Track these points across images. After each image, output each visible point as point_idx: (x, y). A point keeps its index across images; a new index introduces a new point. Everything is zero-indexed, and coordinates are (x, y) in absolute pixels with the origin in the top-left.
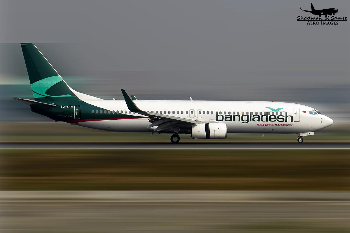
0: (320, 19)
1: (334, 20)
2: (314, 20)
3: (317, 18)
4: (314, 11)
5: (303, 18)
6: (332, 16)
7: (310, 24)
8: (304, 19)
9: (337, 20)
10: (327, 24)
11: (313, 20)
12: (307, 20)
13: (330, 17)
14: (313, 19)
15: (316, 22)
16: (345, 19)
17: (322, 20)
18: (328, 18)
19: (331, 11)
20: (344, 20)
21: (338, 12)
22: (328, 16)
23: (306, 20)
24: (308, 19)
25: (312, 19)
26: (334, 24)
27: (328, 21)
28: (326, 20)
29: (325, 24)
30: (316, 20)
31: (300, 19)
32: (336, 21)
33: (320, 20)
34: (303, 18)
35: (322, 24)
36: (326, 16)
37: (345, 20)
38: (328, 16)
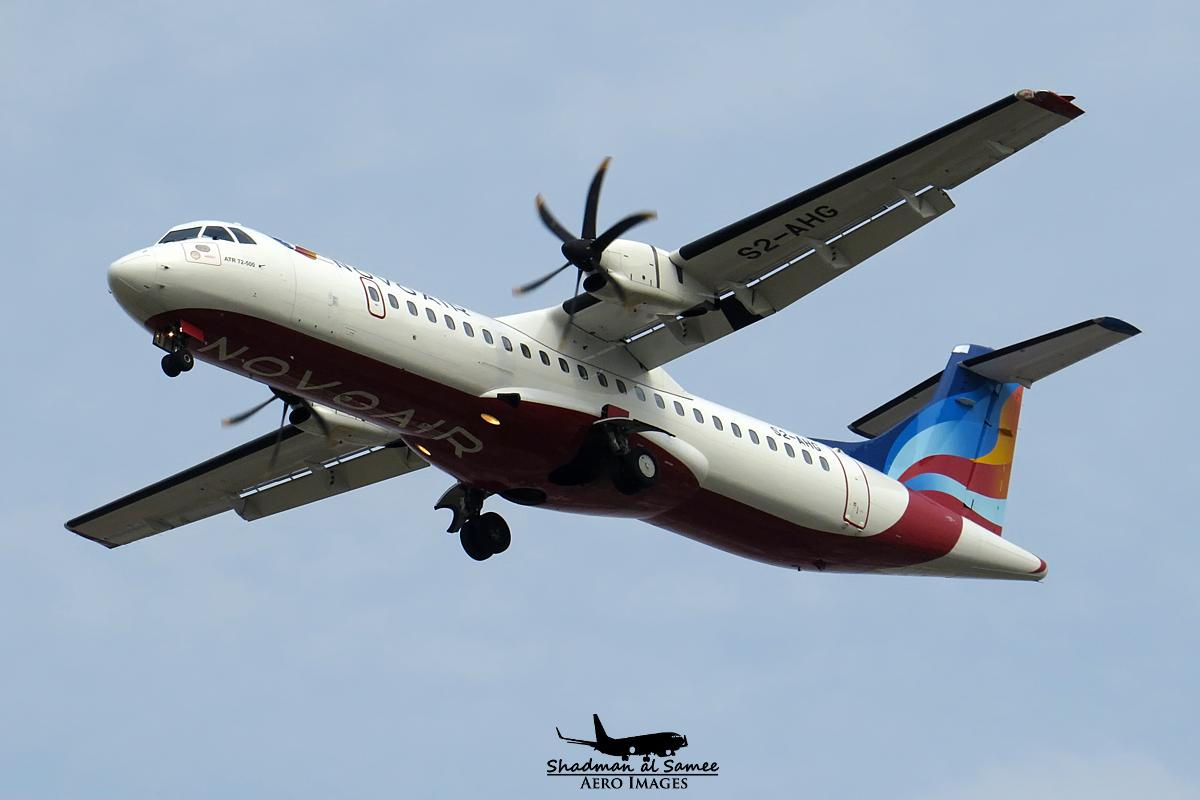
0: (624, 768)
1: (673, 772)
2: (606, 771)
3: (616, 766)
4: (604, 743)
5: (565, 766)
6: (666, 759)
7: (592, 785)
9: (684, 771)
10: (648, 785)
11: (600, 772)
12: (581, 772)
13: (659, 762)
14: (603, 769)
15: (610, 778)
16: (710, 769)
17: (633, 773)
19: (665, 743)
21: (686, 745)
22: (651, 760)
23: (577, 772)
24: (583, 769)
25: (603, 769)
26: (672, 785)
28: (646, 772)
29: (642, 787)
30: (611, 772)
31: (556, 768)
32: (681, 778)
33: (627, 772)
34: (565, 766)
35: (631, 787)
36: (645, 759)
37: (710, 772)
38: (651, 760)
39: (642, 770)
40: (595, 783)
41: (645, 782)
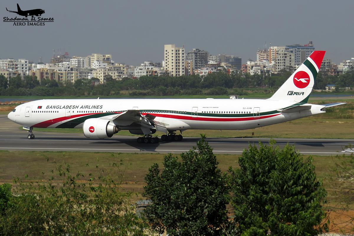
0: (26, 19)
1: (41, 21)
2: (21, 20)
3: (24, 19)
4: (20, 12)
5: (9, 19)
7: (16, 24)
8: (10, 20)
9: (44, 20)
10: (33, 24)
11: (19, 21)
12: (13, 21)
13: (36, 18)
14: (20, 20)
16: (51, 20)
19: (38, 12)
20: (51, 21)
21: (44, 13)
22: (34, 17)
23: (12, 21)
24: (14, 20)
25: (18, 20)
26: (40, 25)
27: (34, 22)
28: (32, 21)
29: (31, 25)
30: (22, 21)
31: (6, 20)
32: (43, 22)
33: (27, 21)
34: (9, 19)
35: (28, 25)
37: (51, 21)
38: (34, 17)
39: (31, 20)
40: (17, 24)
41: (32, 23)
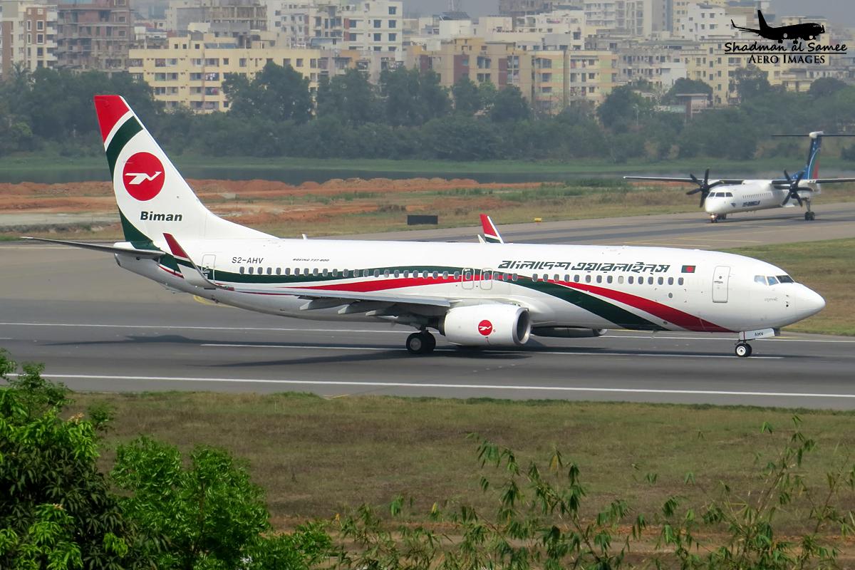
0: (780, 48)
1: (814, 51)
2: (766, 51)
4: (765, 31)
6: (811, 42)
8: (742, 49)
9: (822, 51)
14: (764, 50)
18: (800, 48)
22: (799, 43)
23: (746, 51)
28: (795, 52)
30: (771, 52)
32: (821, 55)
33: (781, 51)
35: (785, 62)
37: (841, 51)
38: (799, 43)
41: (795, 58)
